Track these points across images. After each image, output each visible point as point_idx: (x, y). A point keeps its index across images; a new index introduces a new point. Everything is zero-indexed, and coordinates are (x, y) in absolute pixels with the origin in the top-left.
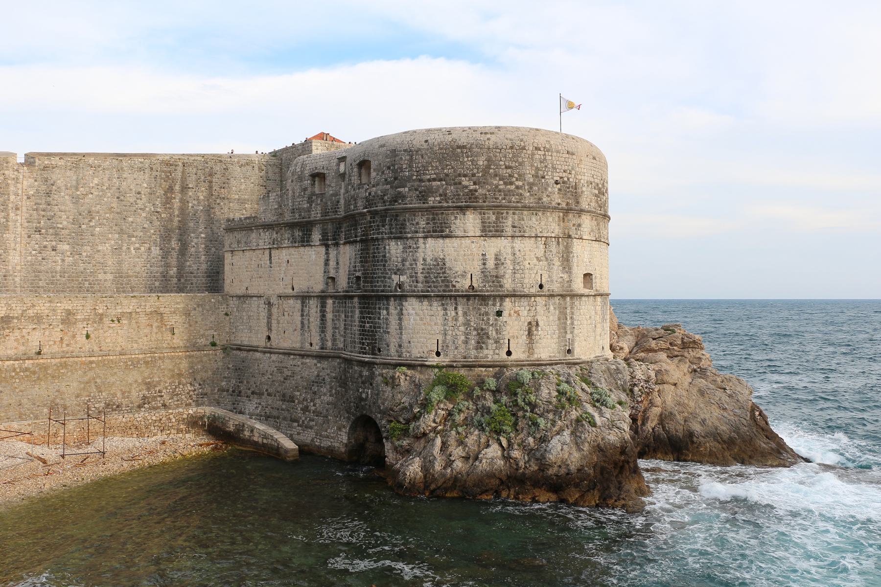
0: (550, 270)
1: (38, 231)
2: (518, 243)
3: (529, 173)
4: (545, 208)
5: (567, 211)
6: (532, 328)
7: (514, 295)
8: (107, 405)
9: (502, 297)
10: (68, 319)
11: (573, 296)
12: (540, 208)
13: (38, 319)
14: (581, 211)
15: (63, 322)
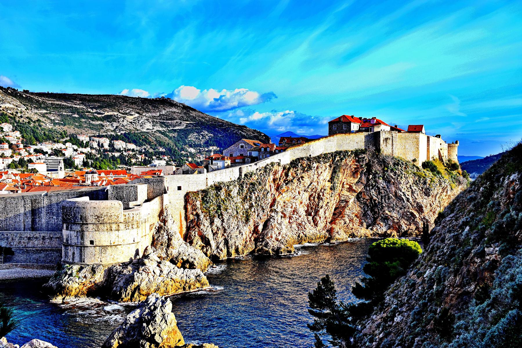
0: (78, 239)
1: (48, 213)
2: (71, 232)
3: (73, 213)
4: (76, 224)
5: (83, 224)
6: (74, 253)
7: (71, 246)
8: (50, 261)
9: (68, 246)
10: (44, 239)
11: (84, 247)
12: (75, 223)
13: (37, 238)
14: (87, 224)
15: (43, 239)
